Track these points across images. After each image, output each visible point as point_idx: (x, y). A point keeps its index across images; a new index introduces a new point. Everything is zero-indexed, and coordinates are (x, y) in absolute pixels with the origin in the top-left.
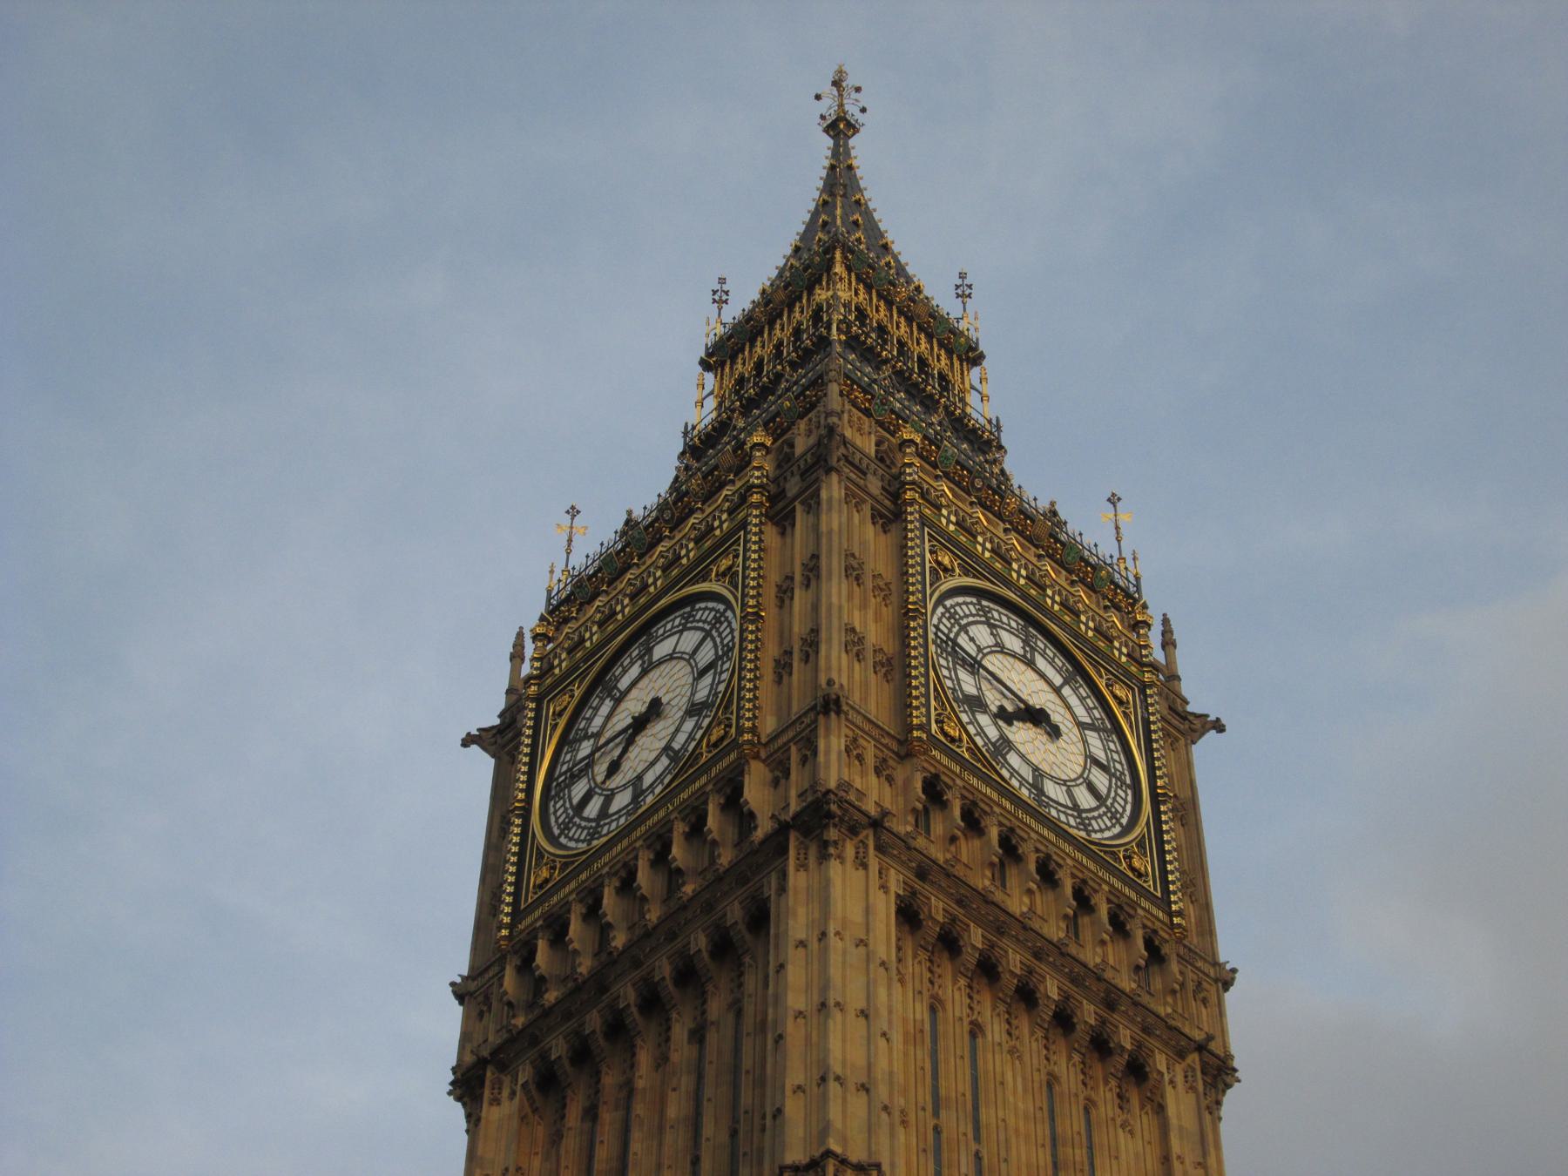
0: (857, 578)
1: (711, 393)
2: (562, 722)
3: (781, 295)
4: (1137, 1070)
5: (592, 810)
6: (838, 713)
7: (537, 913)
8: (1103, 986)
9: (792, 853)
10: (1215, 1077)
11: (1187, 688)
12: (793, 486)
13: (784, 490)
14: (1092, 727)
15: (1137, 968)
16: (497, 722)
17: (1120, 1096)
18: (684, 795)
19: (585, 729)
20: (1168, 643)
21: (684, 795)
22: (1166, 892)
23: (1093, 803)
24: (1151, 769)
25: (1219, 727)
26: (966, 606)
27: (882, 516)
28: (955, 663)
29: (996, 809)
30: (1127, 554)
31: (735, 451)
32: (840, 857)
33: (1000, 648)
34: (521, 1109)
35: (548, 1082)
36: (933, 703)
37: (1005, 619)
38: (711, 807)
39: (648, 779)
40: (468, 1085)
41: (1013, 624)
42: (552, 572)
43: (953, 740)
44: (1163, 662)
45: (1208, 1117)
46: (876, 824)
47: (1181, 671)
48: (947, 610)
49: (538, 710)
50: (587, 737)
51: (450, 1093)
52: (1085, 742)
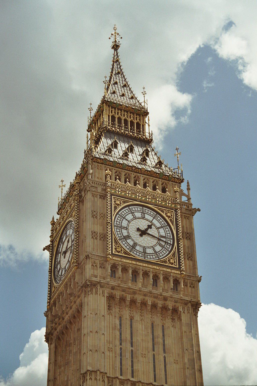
0: (96, 217)
4: (175, 310)
5: (60, 273)
6: (89, 258)
7: (53, 299)
10: (196, 307)
11: (192, 201)
13: (82, 195)
15: (171, 289)
17: (172, 319)
18: (69, 276)
19: (59, 250)
20: (188, 189)
21: (69, 276)
22: (180, 265)
23: (161, 248)
24: (177, 232)
25: (199, 210)
26: (126, 210)
27: (102, 196)
28: (121, 229)
29: (131, 265)
31: (83, 170)
32: (92, 293)
33: (135, 218)
34: (55, 345)
36: (114, 244)
37: (136, 209)
39: (67, 268)
41: (139, 209)
45: (194, 317)
47: (191, 197)
48: (120, 215)
50: (59, 253)
51: (45, 341)
52: (159, 232)
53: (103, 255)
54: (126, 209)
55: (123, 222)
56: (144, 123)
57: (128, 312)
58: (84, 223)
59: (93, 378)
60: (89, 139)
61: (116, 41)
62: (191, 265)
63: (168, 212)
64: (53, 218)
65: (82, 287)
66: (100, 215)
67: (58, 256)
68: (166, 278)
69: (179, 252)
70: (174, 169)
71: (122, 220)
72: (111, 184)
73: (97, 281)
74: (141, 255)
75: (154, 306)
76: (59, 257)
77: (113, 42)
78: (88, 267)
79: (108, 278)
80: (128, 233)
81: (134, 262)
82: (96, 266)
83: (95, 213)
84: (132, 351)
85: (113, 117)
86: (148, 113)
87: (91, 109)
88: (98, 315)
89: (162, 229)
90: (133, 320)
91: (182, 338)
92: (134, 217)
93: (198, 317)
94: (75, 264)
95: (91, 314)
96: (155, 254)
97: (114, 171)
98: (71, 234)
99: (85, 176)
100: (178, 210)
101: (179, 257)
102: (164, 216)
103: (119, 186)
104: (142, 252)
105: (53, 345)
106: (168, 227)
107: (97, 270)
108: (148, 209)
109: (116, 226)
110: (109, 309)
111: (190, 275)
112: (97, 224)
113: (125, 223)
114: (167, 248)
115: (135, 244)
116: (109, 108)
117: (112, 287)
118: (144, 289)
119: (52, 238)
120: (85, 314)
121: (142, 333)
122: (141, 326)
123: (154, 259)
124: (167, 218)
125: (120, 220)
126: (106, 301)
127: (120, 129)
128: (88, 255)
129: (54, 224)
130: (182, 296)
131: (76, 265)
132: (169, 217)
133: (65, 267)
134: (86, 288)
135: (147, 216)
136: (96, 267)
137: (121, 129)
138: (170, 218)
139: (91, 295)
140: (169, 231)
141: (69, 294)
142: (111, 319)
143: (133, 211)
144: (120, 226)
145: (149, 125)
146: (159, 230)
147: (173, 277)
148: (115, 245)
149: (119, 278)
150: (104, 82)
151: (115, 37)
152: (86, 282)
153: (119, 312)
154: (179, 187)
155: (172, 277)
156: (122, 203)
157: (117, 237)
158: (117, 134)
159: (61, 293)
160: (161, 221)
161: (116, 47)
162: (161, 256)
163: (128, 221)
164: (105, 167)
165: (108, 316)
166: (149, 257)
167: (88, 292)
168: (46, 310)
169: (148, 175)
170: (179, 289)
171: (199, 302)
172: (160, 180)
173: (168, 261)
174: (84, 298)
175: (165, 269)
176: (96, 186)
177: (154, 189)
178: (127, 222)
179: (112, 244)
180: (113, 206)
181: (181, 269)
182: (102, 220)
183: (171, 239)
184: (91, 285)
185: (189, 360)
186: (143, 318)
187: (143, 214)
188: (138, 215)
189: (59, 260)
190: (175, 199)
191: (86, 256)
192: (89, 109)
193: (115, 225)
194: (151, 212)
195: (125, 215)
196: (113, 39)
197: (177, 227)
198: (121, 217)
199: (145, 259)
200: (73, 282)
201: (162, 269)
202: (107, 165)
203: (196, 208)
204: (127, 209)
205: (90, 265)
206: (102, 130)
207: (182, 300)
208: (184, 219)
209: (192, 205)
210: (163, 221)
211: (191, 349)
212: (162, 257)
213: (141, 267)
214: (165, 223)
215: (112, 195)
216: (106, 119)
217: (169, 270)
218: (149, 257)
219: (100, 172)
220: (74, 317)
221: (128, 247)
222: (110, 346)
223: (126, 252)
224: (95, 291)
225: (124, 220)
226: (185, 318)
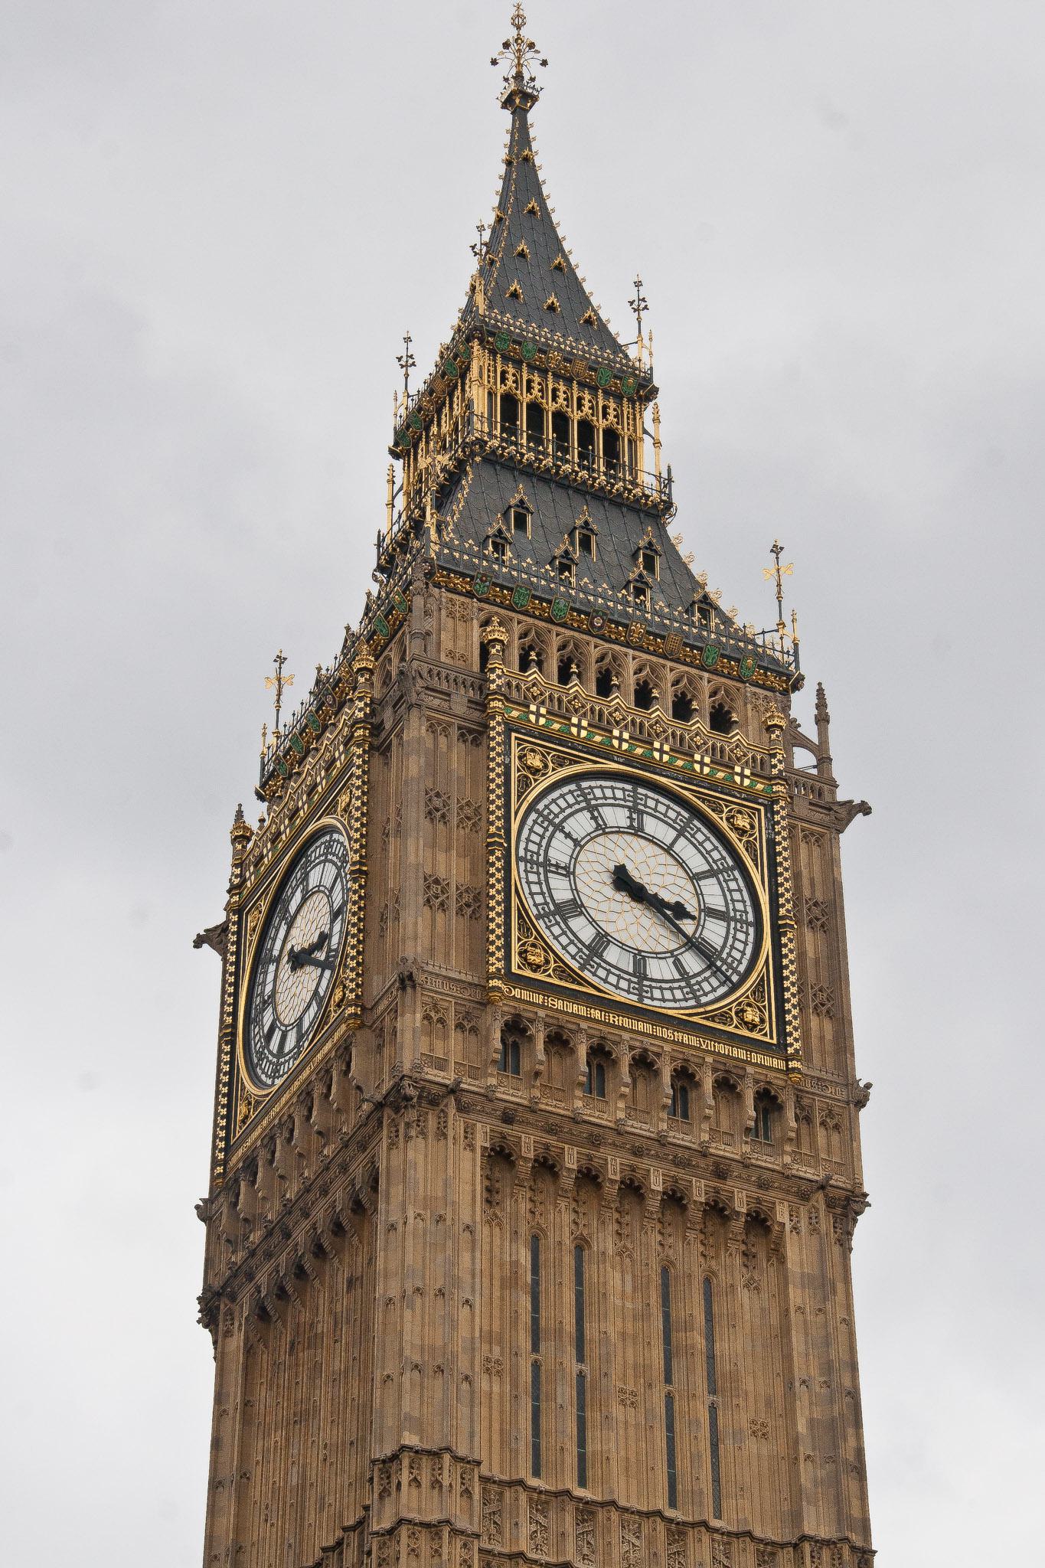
0: (443, 816)
1: (401, 489)
2: (255, 938)
3: (440, 386)
4: (759, 1222)
6: (414, 987)
7: (240, 1152)
8: (711, 1160)
9: (385, 1132)
11: (837, 771)
12: (388, 717)
14: (711, 873)
15: (748, 1130)
16: (220, 918)
17: (744, 1254)
18: (319, 1056)
19: (271, 950)
21: (319, 1056)
22: (783, 1034)
25: (865, 809)
26: (567, 795)
27: (470, 731)
28: (546, 872)
29: (584, 1025)
30: (787, 619)
31: (386, 617)
32: (423, 1133)
33: (602, 829)
34: (247, 1338)
35: (262, 1314)
36: (515, 933)
37: (608, 793)
38: (335, 1074)
39: (306, 1024)
40: (213, 1309)
41: (619, 794)
42: (264, 734)
43: (536, 968)
44: (815, 740)
45: (836, 1249)
46: (453, 1090)
47: (833, 753)
48: (540, 814)
49: (239, 923)
50: (271, 961)
51: (199, 1322)
52: (699, 894)
53: (469, 979)
54: (565, 789)
55: (554, 842)
56: (635, 431)
57: (567, 1217)
58: (392, 840)
59: (425, 1480)
60: (396, 487)
61: (519, 76)
62: (829, 1036)
63: (739, 812)
64: (240, 814)
65: (379, 1106)
66: (461, 808)
67: (266, 973)
68: (726, 1086)
69: (779, 979)
70: (763, 633)
71: (548, 834)
72: (509, 684)
73: (447, 1082)
74: (624, 984)
75: (675, 1199)
76: (270, 977)
77: (506, 80)
78: (411, 1021)
79: (491, 1075)
80: (575, 890)
81: (596, 1014)
82: (441, 1021)
83: (437, 802)
84: (581, 1376)
85: (510, 402)
86: (655, 390)
87: (407, 363)
88: (449, 1222)
89: (714, 880)
90: (586, 1253)
91: (785, 1331)
92: (598, 825)
93: (850, 1249)
94: (351, 1010)
95: (418, 1220)
96: (683, 984)
97: (517, 629)
98: (328, 882)
99: (392, 645)
100: (782, 803)
101: (781, 1001)
102: (724, 825)
103: (541, 694)
104: (631, 970)
105: (236, 1342)
106: (737, 873)
107: (446, 1037)
108: (656, 797)
109: (526, 861)
110: (488, 1201)
111: (823, 1075)
112: (448, 849)
113: (560, 851)
114: (730, 960)
115: (603, 939)
116: (495, 360)
117: (504, 1113)
118: (635, 1126)
119: (236, 898)
120: (392, 1219)
121: (623, 1307)
122: (618, 1275)
123: (677, 1005)
124: (733, 836)
125: (542, 837)
126: (478, 1169)
127: (539, 452)
128: (411, 977)
129: (249, 839)
130: (787, 1159)
131: (356, 1014)
132: (742, 832)
133: (301, 1019)
134: (397, 1110)
135: (651, 826)
136: (440, 1026)
137: (543, 453)
138: (745, 839)
139: (420, 1140)
140: (740, 891)
141: (319, 1133)
142: (497, 1241)
143: (593, 802)
144: (541, 859)
145: (657, 443)
146: (701, 883)
147: (757, 1081)
148: (519, 940)
149: (537, 1074)
150: (473, 247)
151: (519, 58)
152: (397, 1087)
153: (529, 1216)
154: (786, 708)
155: (749, 1082)
156: (551, 765)
157: (529, 903)
158: (530, 472)
159: (281, 1125)
160: (708, 846)
161: (520, 100)
162: (706, 994)
163: (576, 843)
164: (481, 610)
165: (486, 1230)
166: (657, 994)
167: (408, 1125)
168: (206, 1196)
169: (654, 653)
170: (777, 1133)
171: (857, 1191)
172: (706, 675)
173: (737, 1013)
174: (389, 1149)
175: (723, 1049)
176: (444, 686)
177: (682, 709)
178: (570, 843)
179: (507, 935)
180: (514, 775)
181: (790, 1050)
182: (467, 830)
183: (749, 924)
184: (420, 1097)
185: (812, 1423)
186: (630, 1246)
187: (635, 816)
188: (617, 817)
189: (269, 988)
190: (766, 758)
191: (402, 981)
192: (399, 359)
193: (522, 853)
194: (668, 807)
195: (561, 817)
196: (506, 67)
197: (774, 875)
198: (546, 824)
199: (640, 1001)
200: (338, 1083)
201: (711, 1045)
202: (486, 601)
203: (851, 802)
204: (571, 792)
205: (419, 1016)
206: (463, 451)
207: (787, 1177)
208: (803, 845)
209: (837, 786)
210: (716, 848)
211: (823, 1379)
212: (711, 997)
213: (626, 1036)
214: (723, 858)
215: (509, 729)
216: (480, 406)
217: (741, 1054)
218: (657, 994)
219: (460, 631)
220: (338, 1229)
221: (572, 949)
222: (491, 1350)
223: (564, 971)
224: (435, 1125)
225: (559, 835)
226: (798, 1253)
